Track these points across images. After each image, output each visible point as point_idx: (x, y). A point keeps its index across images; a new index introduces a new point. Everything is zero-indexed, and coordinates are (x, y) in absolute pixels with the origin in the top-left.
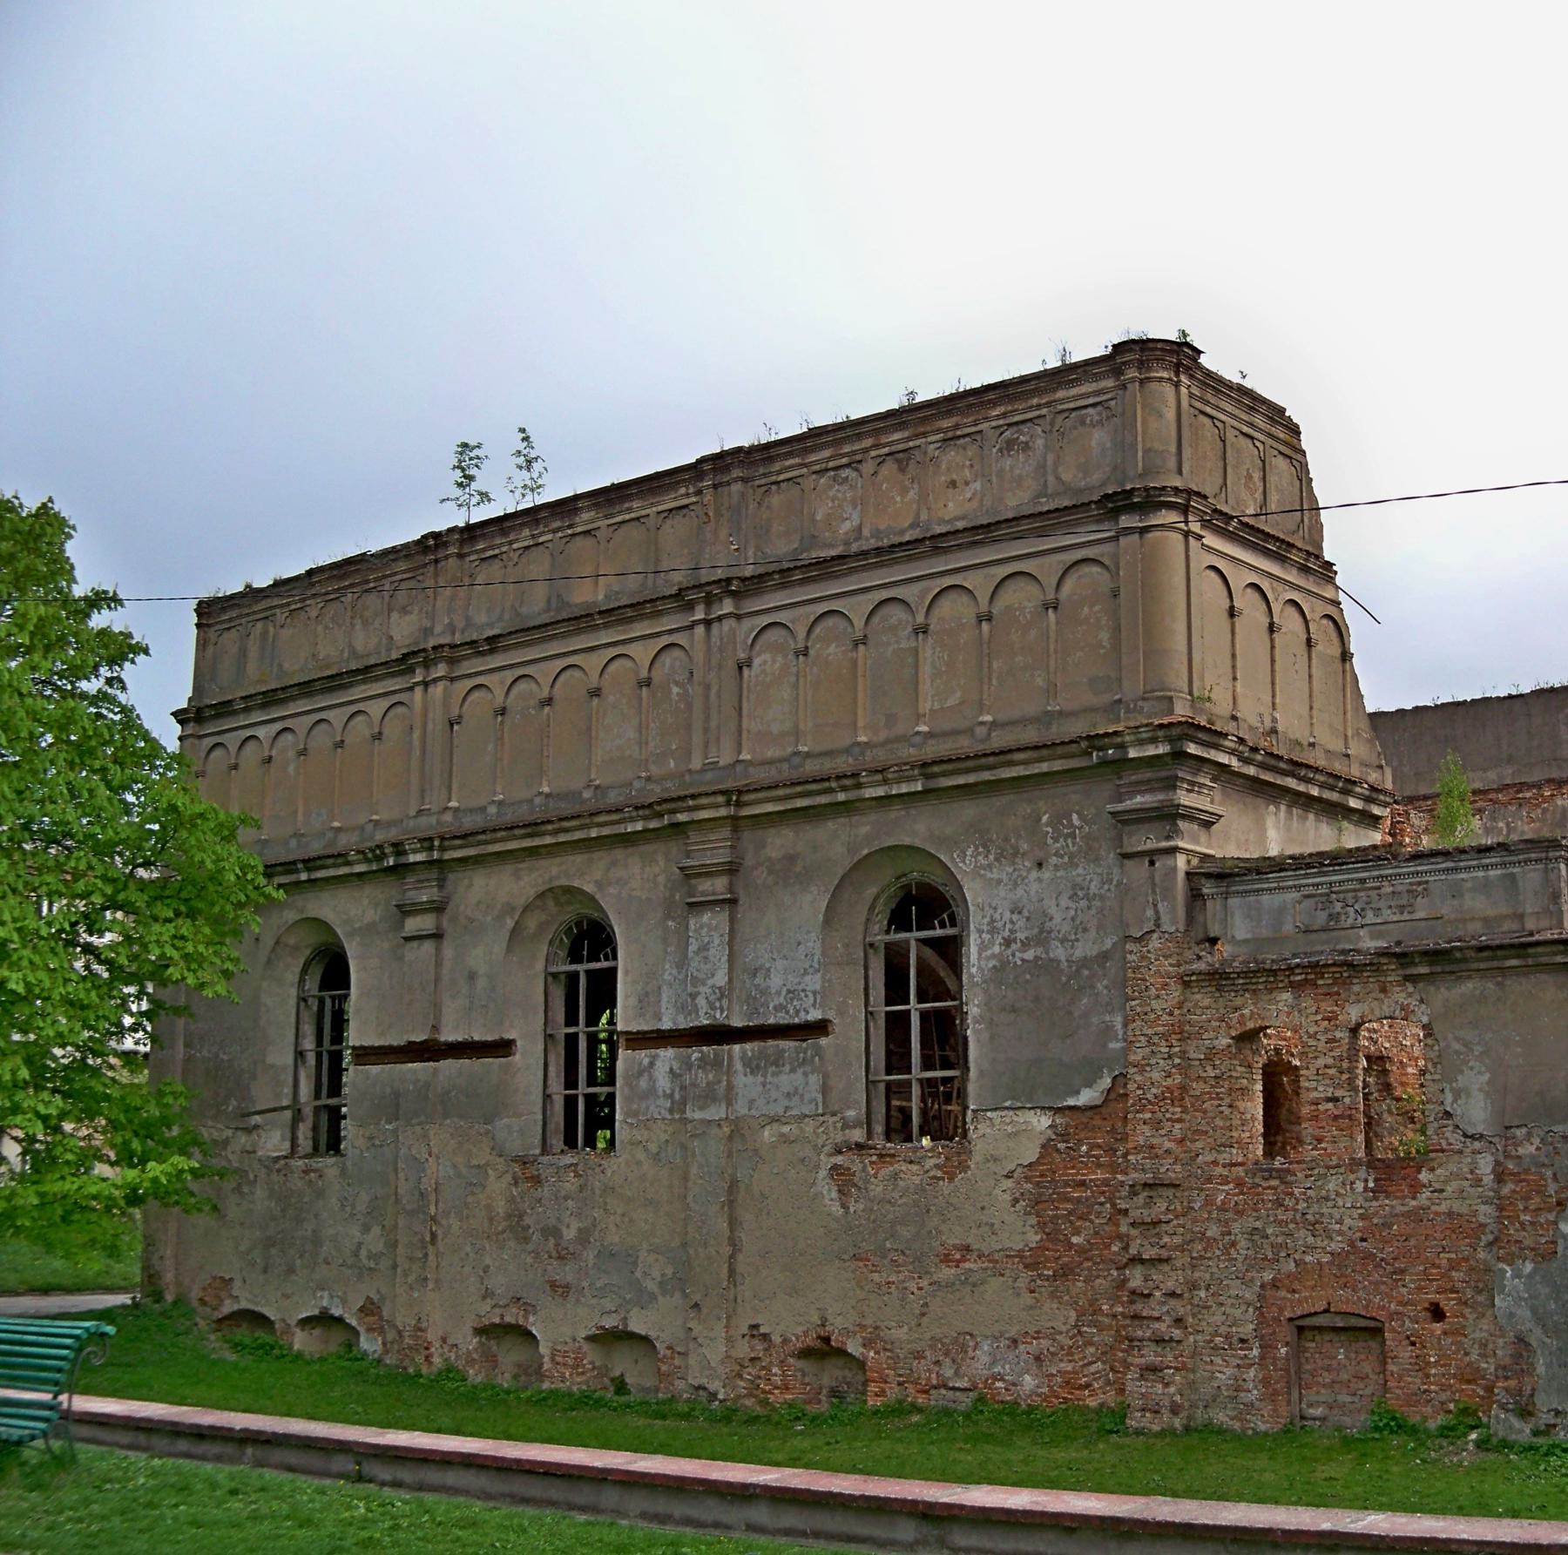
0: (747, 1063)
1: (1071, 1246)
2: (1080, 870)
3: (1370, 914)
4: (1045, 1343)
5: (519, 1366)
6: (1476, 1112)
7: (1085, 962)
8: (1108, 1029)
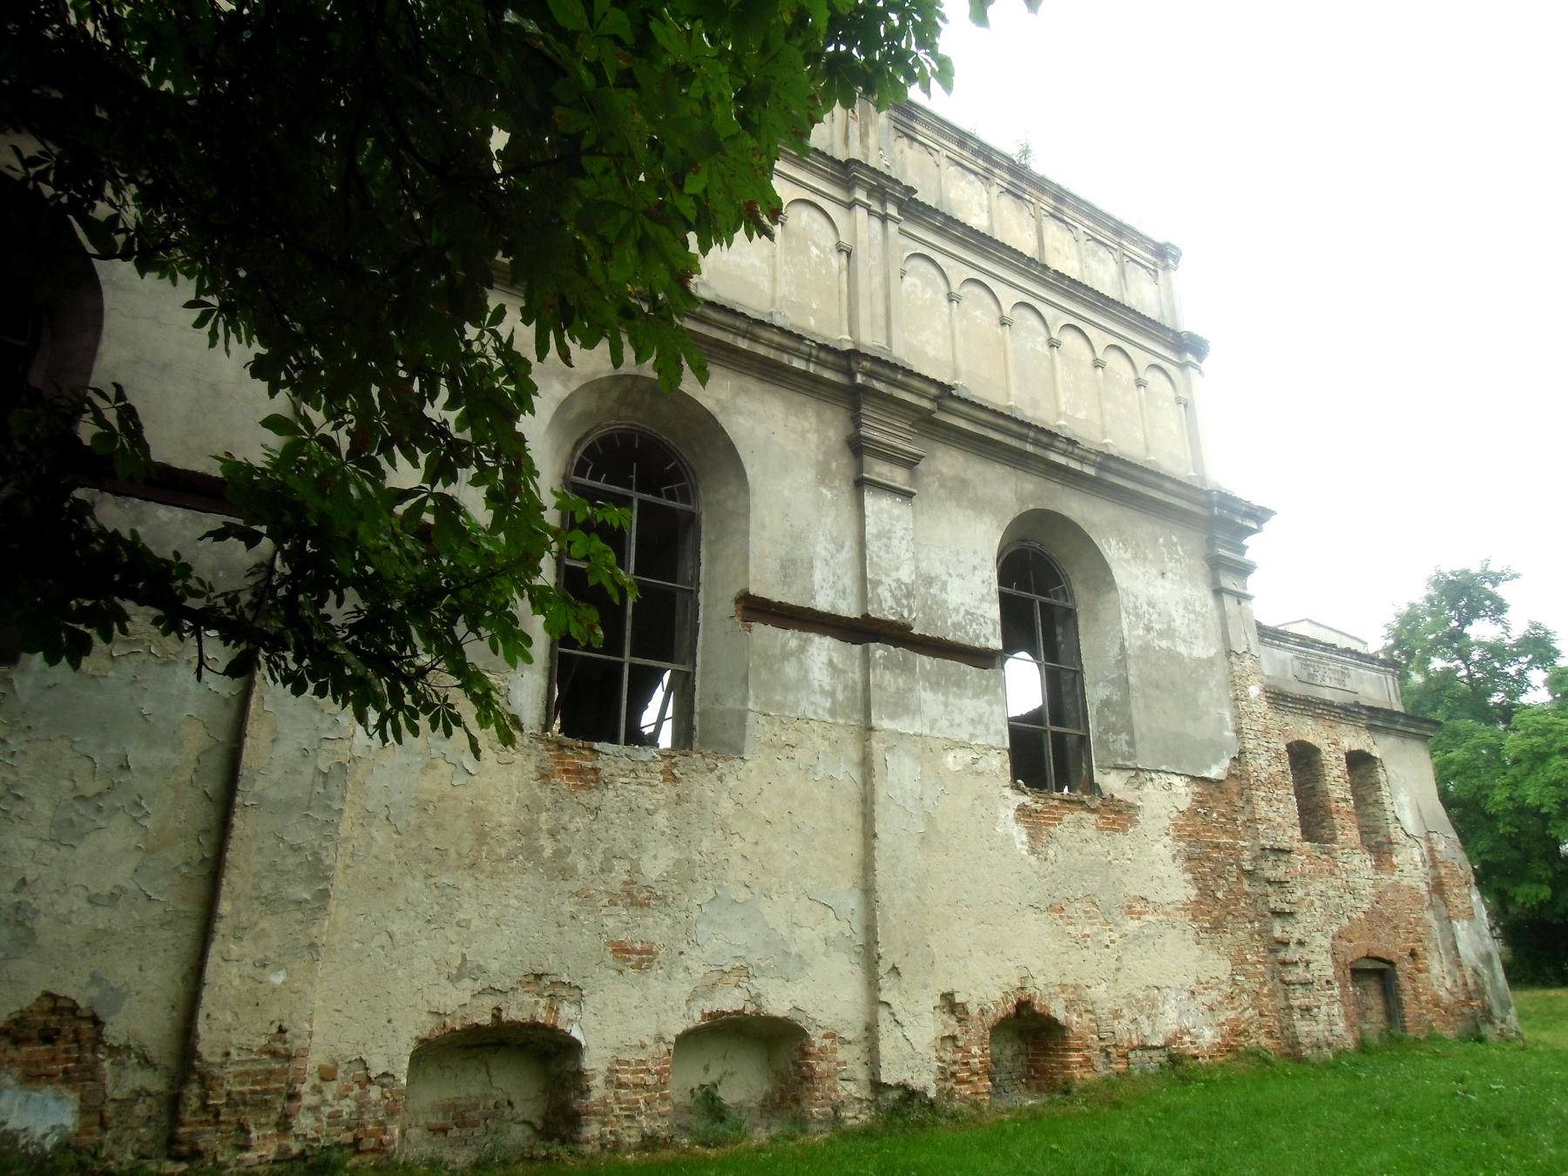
4: (1214, 993)
5: (448, 1108)
8: (1221, 720)
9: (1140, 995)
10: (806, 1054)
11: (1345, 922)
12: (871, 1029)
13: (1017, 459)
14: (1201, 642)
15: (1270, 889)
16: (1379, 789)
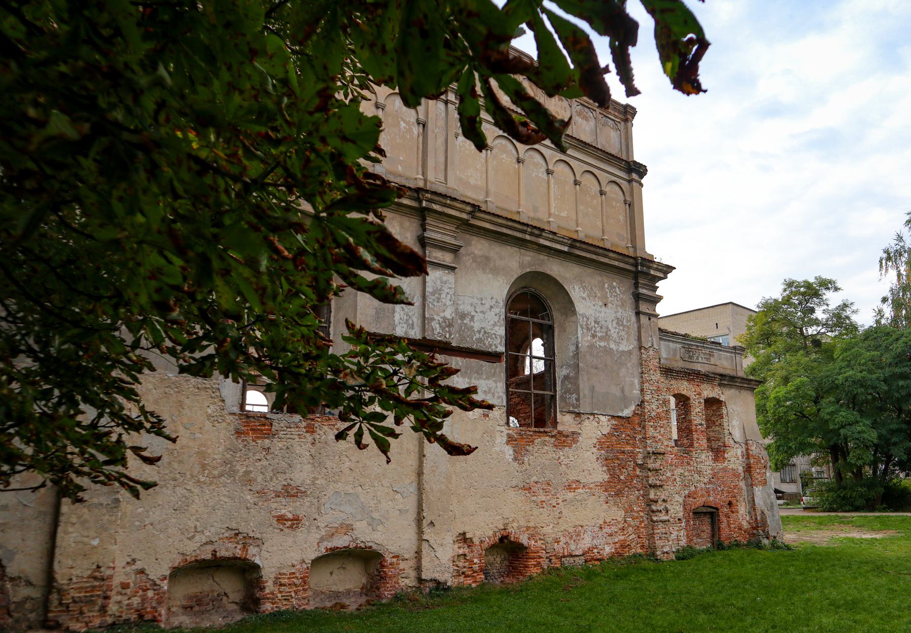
1: (620, 480)
5: (190, 598)
6: (737, 435)
8: (633, 384)
9: (571, 530)
10: (383, 566)
11: (693, 488)
12: (418, 554)
13: (521, 243)
14: (625, 342)
15: (650, 474)
16: (722, 418)
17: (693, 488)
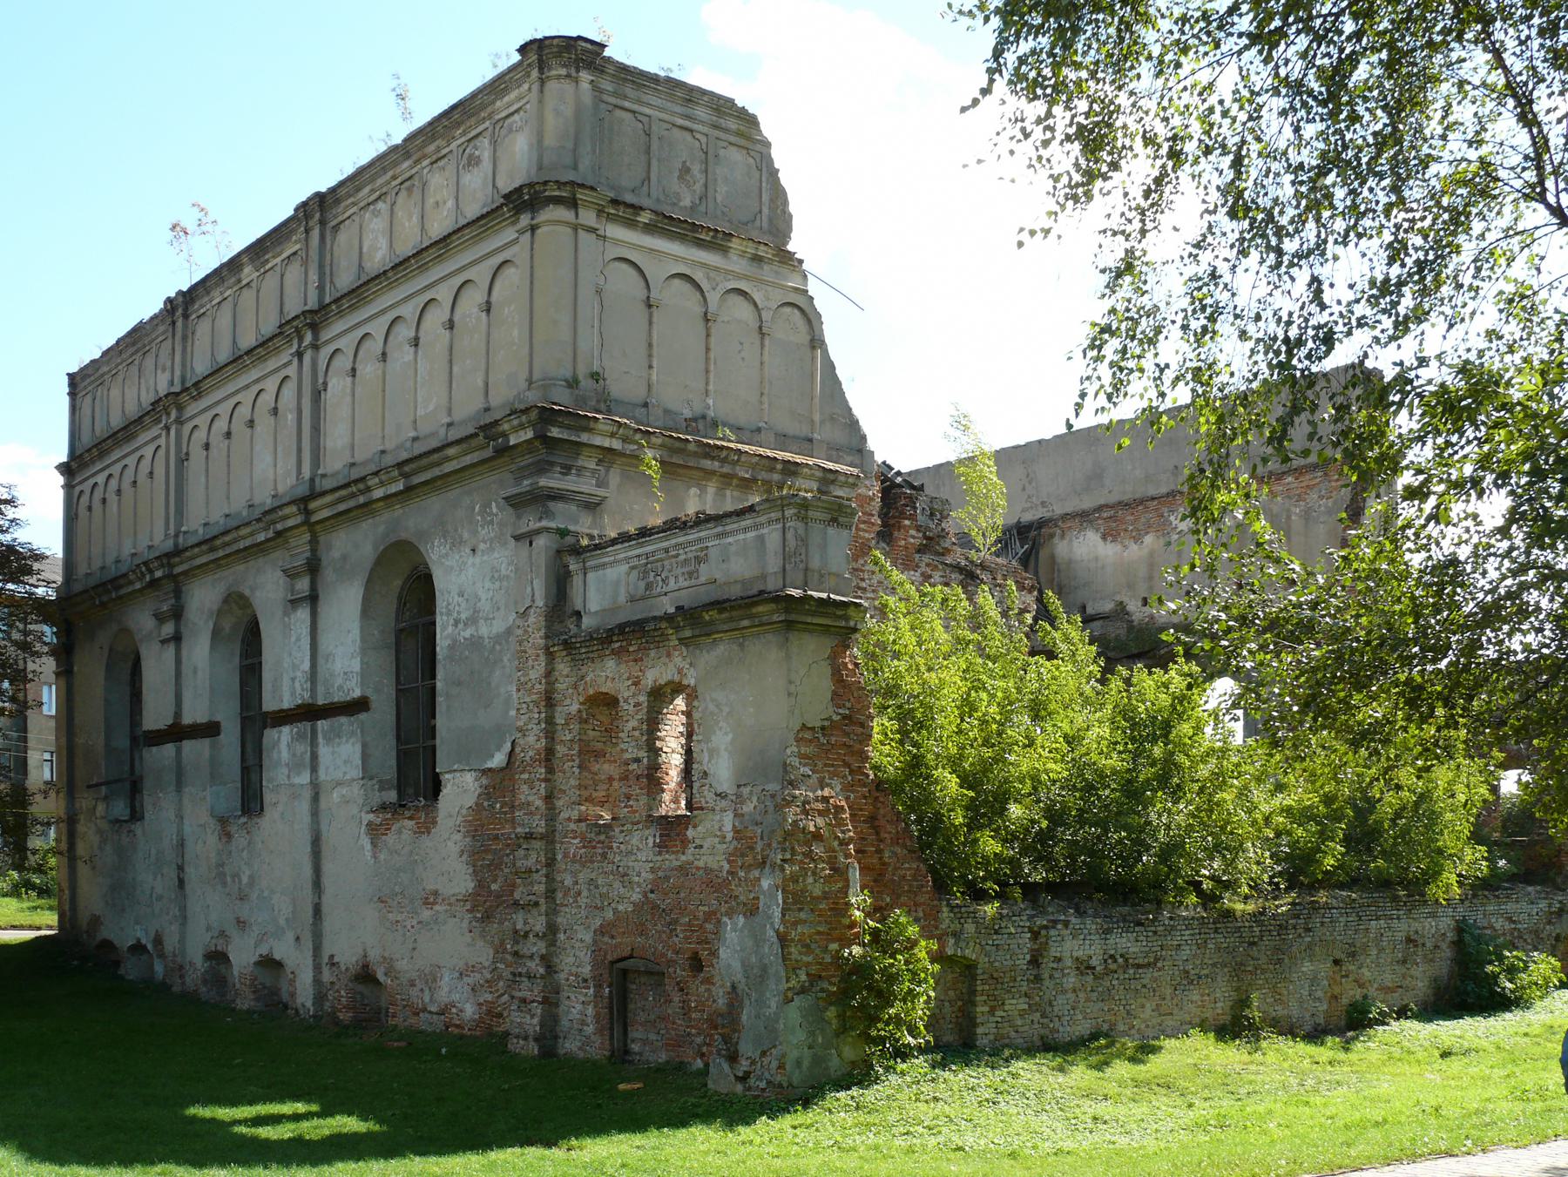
0: (324, 738)
1: (490, 892)
2: (496, 555)
3: (672, 581)
7: (498, 636)
11: (609, 915)
17: (609, 915)
